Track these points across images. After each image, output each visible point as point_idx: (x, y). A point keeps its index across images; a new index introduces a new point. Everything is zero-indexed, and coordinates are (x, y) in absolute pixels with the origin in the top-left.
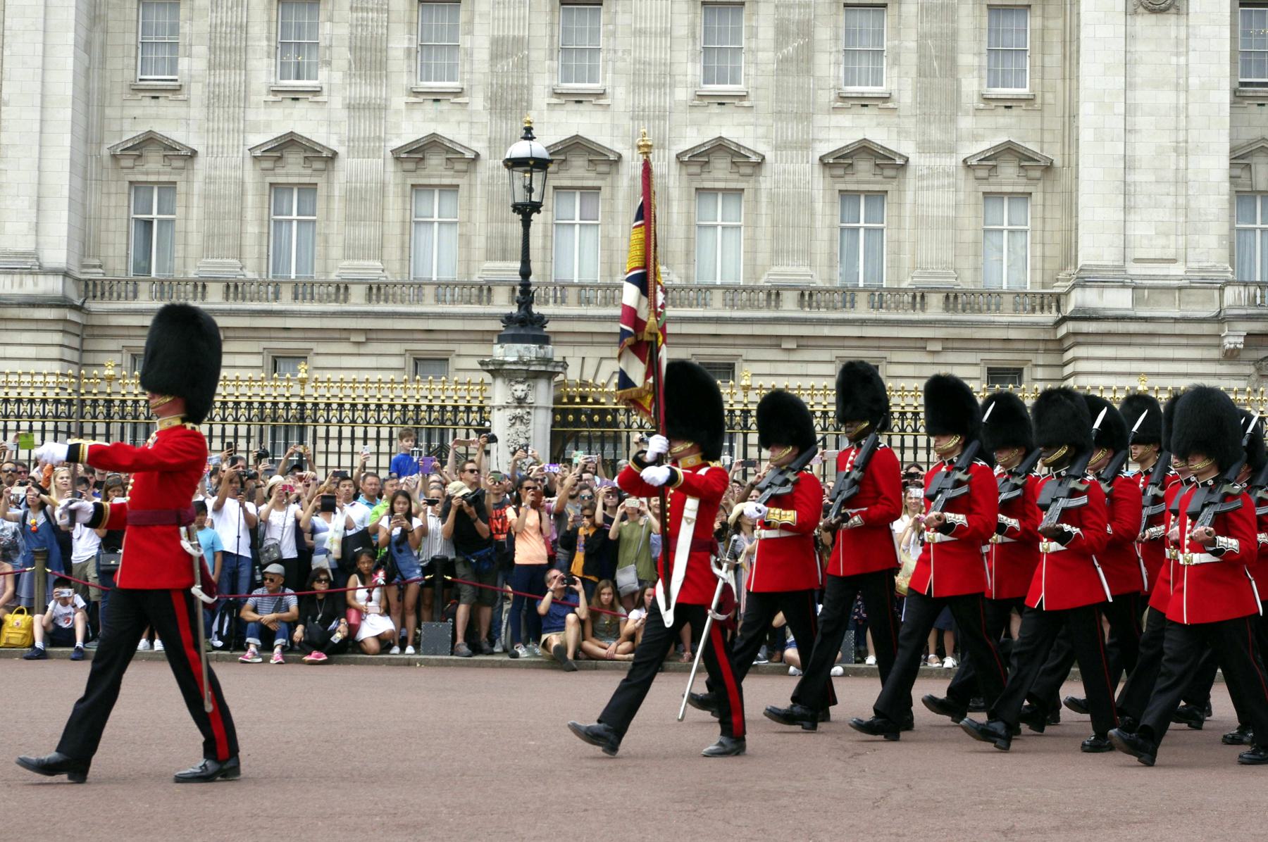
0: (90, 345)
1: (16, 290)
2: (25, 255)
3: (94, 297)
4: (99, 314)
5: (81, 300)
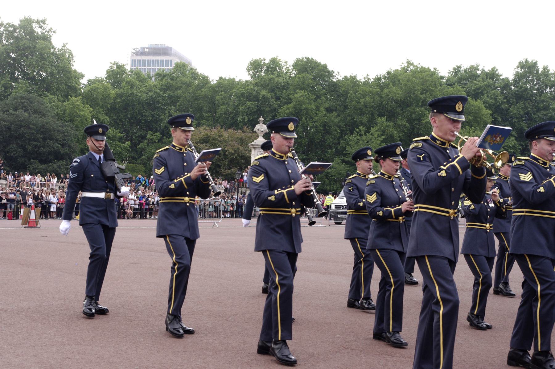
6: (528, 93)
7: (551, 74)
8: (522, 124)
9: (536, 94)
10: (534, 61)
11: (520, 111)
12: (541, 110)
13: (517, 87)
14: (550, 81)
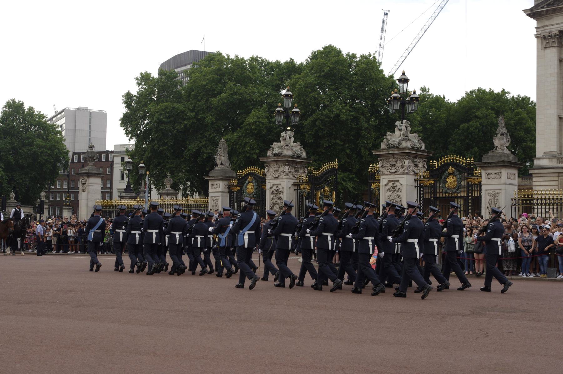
6: (15, 130)
7: (36, 115)
8: (9, 157)
9: (22, 131)
10: (21, 103)
11: (7, 146)
12: (26, 145)
13: (5, 124)
14: (35, 121)
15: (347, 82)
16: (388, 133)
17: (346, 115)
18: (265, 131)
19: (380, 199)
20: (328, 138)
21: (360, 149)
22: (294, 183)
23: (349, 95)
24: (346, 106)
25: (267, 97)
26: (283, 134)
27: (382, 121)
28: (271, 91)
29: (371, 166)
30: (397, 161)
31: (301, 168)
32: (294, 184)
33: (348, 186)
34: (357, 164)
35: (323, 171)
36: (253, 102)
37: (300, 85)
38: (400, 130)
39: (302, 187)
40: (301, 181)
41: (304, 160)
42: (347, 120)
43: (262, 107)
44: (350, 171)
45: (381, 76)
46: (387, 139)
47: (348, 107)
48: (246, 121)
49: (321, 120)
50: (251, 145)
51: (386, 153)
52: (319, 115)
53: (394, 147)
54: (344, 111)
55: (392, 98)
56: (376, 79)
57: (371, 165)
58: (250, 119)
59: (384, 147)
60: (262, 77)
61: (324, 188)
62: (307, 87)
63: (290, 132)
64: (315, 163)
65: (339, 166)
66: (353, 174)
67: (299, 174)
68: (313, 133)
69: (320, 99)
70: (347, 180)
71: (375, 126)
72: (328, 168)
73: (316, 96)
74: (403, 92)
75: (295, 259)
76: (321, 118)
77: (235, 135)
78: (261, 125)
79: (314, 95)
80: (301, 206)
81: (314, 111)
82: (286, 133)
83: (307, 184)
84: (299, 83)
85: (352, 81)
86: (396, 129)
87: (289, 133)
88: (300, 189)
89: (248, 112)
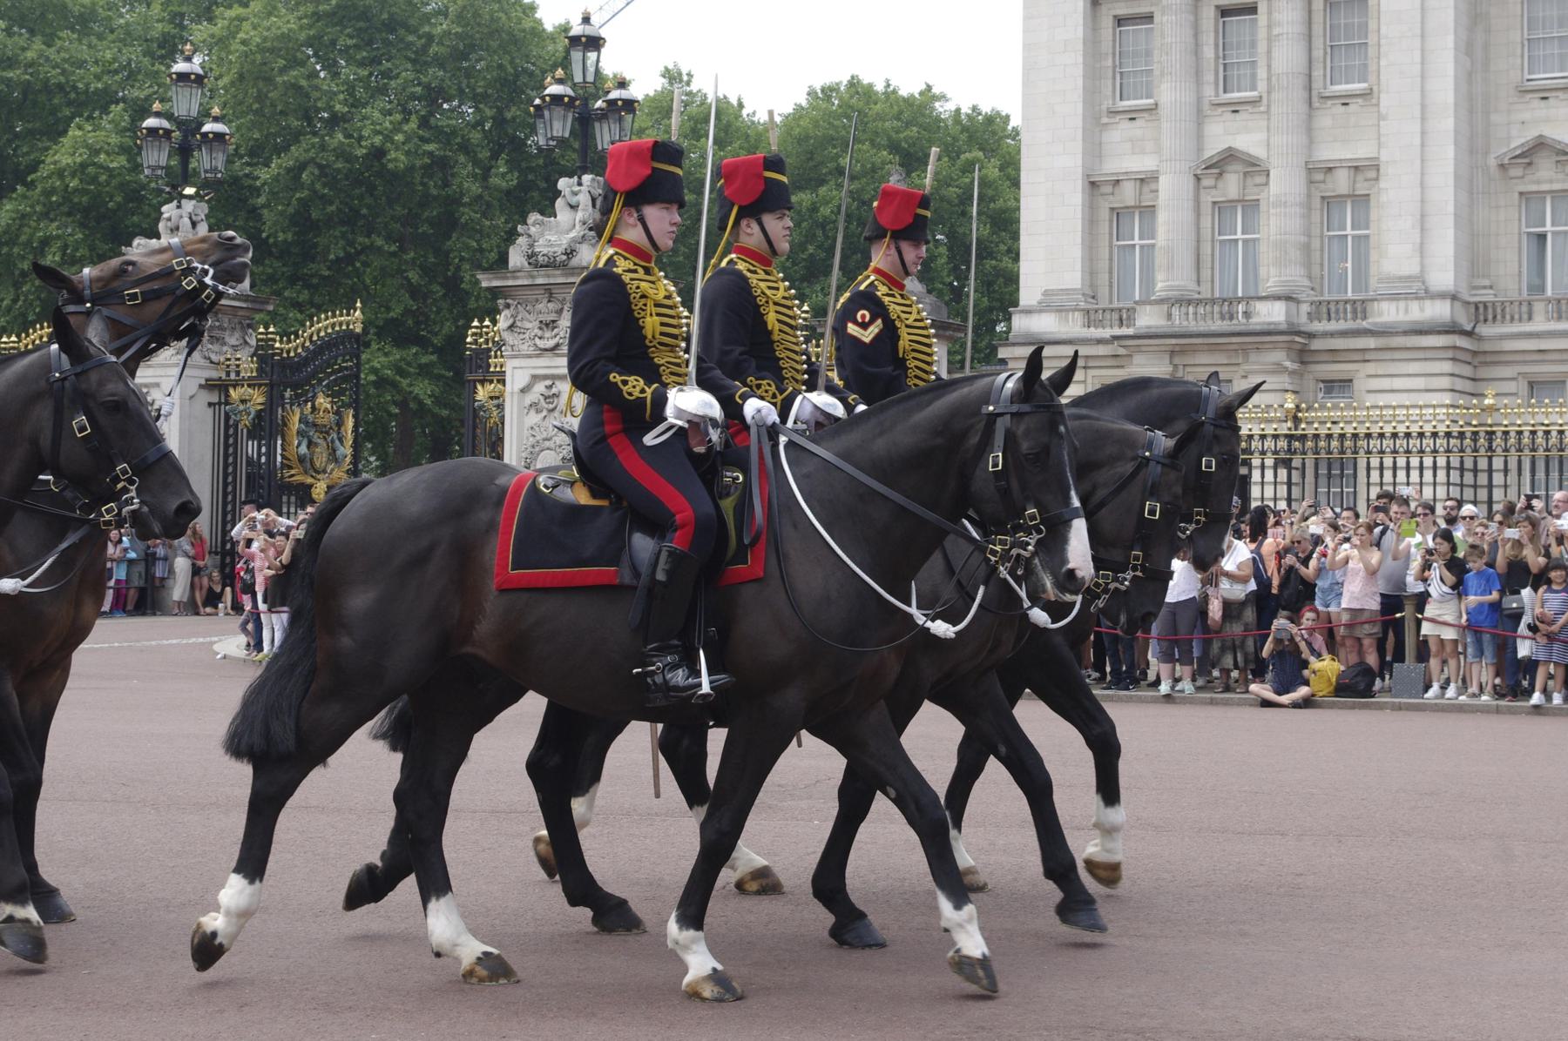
0: (1483, 372)
1: (1402, 317)
2: (1409, 279)
3: (1486, 320)
4: (1491, 339)
5: (1472, 325)
15: (411, 38)
16: (534, 217)
17: (408, 153)
18: (119, 199)
19: (501, 440)
20: (344, 229)
21: (458, 268)
22: (207, 380)
23: (419, 84)
24: (407, 121)
25: (128, 77)
26: (168, 210)
27: (530, 177)
28: (141, 58)
29: (476, 327)
30: (562, 309)
31: (233, 329)
32: (209, 385)
33: (416, 390)
34: (447, 320)
35: (311, 341)
36: (73, 95)
37: (244, 42)
38: (574, 207)
39: (234, 394)
40: (233, 376)
41: (246, 301)
42: (411, 169)
43: (108, 113)
44: (423, 343)
45: (527, 24)
46: (530, 236)
47: (413, 125)
48: (49, 160)
49: (320, 167)
50: (66, 246)
51: (526, 283)
52: (314, 147)
53: (551, 264)
54: (399, 137)
55: (548, 99)
56: (511, 34)
57: (476, 323)
58: (64, 154)
59: (519, 264)
60: (109, 10)
61: (314, 397)
62: (272, 50)
63: (193, 202)
64: (298, 315)
65: (367, 324)
66: (432, 353)
67: (225, 348)
68: (291, 210)
69: (315, 94)
70: (412, 370)
71: (508, 193)
72: (330, 331)
73: (303, 83)
74: (585, 82)
75: (203, 644)
76: (318, 160)
77: (7, 211)
78: (103, 178)
79: (295, 77)
80: (231, 460)
81: (296, 137)
82: (179, 207)
83: (254, 385)
84: (241, 35)
85: (430, 38)
86: (559, 203)
87: (188, 206)
88: (227, 403)
89: (56, 131)
